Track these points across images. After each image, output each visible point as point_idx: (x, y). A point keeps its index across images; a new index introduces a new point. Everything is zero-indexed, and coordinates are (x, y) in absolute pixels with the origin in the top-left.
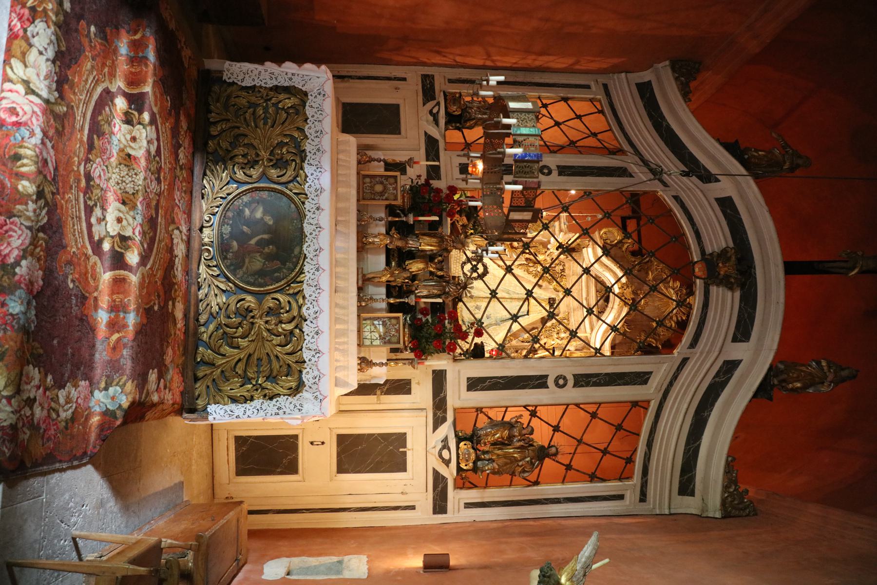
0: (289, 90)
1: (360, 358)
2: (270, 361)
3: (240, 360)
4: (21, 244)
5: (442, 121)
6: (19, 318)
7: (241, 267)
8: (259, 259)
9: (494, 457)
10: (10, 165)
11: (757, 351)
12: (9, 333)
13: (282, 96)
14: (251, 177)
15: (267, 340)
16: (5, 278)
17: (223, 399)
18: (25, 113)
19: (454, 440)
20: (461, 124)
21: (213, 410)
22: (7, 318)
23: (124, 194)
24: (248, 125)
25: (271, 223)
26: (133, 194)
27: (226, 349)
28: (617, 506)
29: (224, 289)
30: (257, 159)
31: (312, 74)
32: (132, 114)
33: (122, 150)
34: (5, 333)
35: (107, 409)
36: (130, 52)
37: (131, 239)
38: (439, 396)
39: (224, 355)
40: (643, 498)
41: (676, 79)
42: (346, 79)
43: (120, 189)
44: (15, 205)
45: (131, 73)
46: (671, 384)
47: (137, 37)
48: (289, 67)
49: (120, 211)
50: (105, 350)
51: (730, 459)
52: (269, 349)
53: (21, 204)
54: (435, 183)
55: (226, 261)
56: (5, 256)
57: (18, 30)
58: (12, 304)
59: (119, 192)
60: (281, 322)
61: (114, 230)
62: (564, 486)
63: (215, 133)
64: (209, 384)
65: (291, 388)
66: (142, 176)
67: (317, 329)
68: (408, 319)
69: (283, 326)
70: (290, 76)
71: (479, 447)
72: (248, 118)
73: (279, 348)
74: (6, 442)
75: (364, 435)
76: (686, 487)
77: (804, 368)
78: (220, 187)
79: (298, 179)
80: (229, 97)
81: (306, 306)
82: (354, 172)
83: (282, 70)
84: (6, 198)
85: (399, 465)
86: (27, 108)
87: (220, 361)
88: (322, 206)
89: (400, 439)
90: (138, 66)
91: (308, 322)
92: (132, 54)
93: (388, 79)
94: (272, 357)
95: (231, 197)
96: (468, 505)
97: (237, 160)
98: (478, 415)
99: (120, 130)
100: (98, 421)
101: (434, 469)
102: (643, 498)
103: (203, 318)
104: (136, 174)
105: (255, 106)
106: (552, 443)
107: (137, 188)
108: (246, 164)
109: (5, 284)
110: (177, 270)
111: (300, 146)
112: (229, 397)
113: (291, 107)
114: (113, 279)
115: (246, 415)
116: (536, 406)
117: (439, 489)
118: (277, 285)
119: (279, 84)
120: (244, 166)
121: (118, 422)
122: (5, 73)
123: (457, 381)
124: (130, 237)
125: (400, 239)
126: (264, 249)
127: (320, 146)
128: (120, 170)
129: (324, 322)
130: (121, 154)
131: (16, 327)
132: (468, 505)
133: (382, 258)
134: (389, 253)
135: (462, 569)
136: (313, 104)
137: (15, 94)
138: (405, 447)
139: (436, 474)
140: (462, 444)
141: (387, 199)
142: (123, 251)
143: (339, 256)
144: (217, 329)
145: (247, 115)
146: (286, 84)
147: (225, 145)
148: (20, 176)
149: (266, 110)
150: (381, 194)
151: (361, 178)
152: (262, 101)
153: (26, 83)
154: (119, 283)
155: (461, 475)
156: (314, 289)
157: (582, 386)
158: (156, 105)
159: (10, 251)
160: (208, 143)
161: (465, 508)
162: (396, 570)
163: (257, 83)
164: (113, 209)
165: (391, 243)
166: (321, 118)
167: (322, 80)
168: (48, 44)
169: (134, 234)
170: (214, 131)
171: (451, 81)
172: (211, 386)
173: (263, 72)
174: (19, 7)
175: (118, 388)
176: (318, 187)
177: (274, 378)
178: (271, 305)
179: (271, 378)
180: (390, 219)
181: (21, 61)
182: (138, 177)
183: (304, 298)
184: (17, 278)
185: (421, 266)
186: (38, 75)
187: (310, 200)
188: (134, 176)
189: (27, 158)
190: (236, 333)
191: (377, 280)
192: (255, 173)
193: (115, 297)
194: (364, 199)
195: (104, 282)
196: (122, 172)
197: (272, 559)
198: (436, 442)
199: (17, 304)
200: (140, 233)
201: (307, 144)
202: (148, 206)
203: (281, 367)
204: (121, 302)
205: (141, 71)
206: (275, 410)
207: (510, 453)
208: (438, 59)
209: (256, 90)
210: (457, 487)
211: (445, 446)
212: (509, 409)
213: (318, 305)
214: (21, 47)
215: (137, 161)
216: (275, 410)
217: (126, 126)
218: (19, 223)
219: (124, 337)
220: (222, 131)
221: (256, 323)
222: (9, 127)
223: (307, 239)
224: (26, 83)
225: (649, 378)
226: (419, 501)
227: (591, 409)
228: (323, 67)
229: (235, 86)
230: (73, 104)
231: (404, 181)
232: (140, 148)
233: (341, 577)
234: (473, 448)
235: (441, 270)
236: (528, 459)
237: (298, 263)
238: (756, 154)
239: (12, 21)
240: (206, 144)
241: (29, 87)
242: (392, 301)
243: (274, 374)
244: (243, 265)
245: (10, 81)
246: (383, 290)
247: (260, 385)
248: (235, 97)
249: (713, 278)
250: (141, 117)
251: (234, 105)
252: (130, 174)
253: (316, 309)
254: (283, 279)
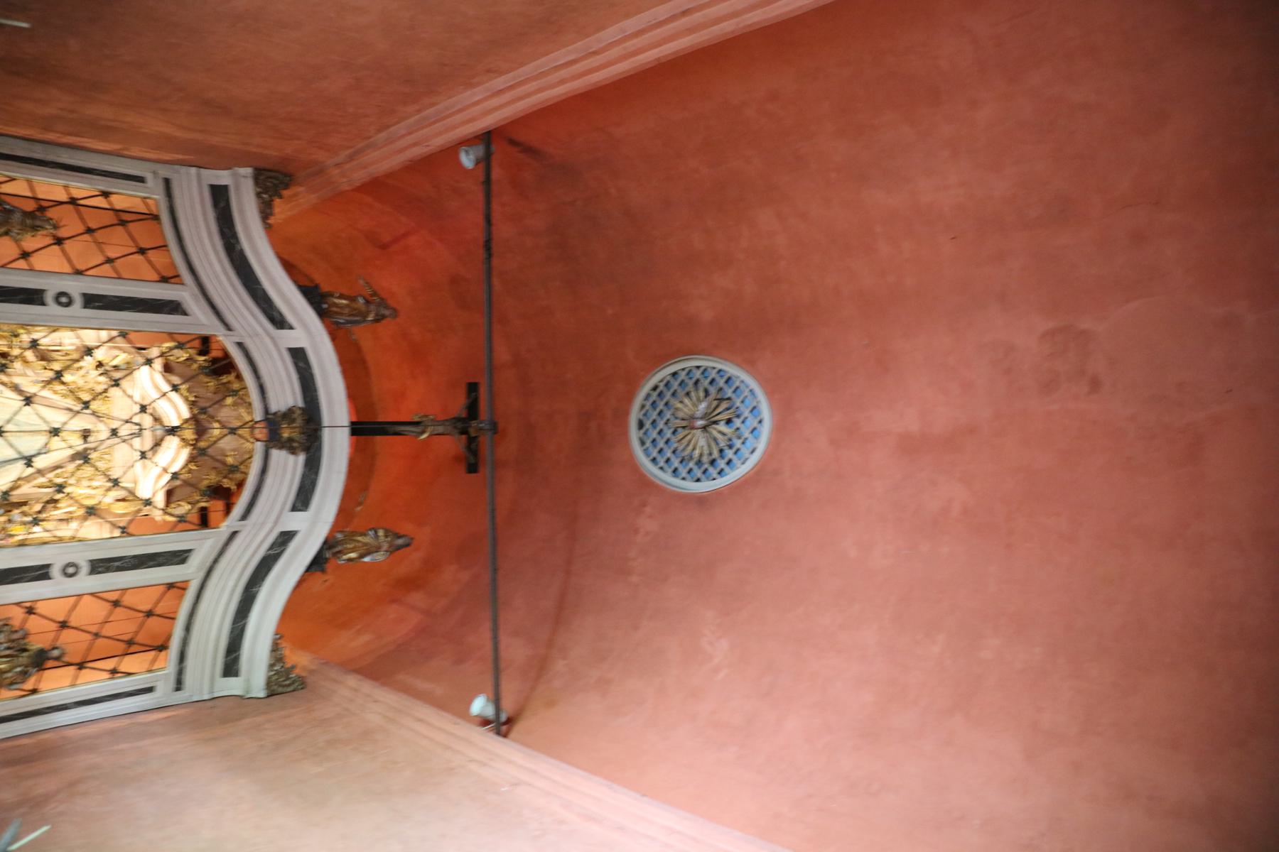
11: (314, 524)
28: (143, 701)
40: (179, 685)
41: (258, 195)
46: (216, 561)
51: (278, 636)
76: (231, 669)
77: (360, 538)
102: (179, 685)
157: (100, 573)
225: (187, 557)
227: (113, 596)
236: (19, 669)
238: (337, 301)
249: (274, 440)
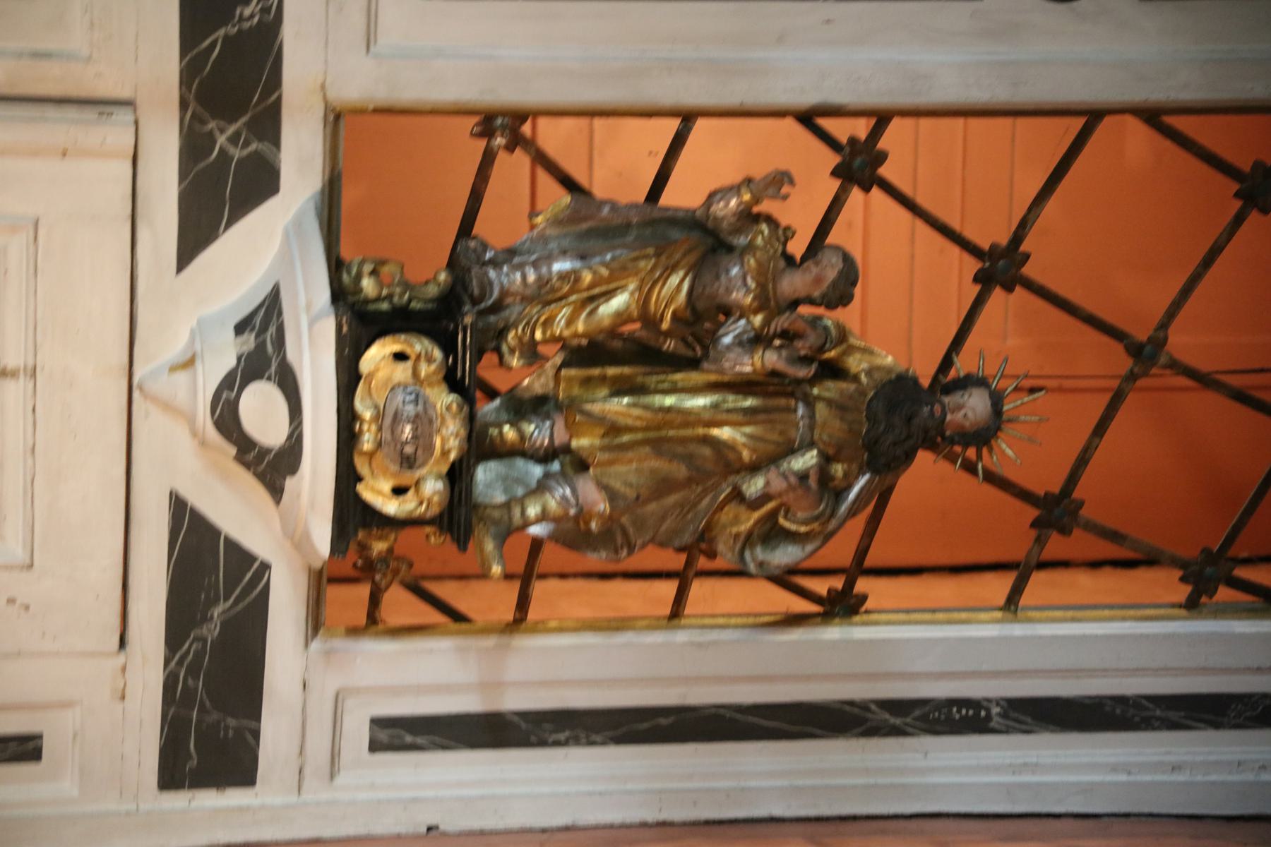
9: (582, 442)
19: (328, 329)
38: (226, 17)
62: (1017, 630)
71: (488, 370)
98: (488, 159)
101: (179, 506)
106: (963, 365)
116: (882, 119)
117: (211, 631)
140: (377, 355)
155: (364, 548)
161: (375, 746)
198: (201, 330)
207: (689, 418)
212: (701, 125)
226: (66, 705)
234: (453, 381)
236: (806, 461)
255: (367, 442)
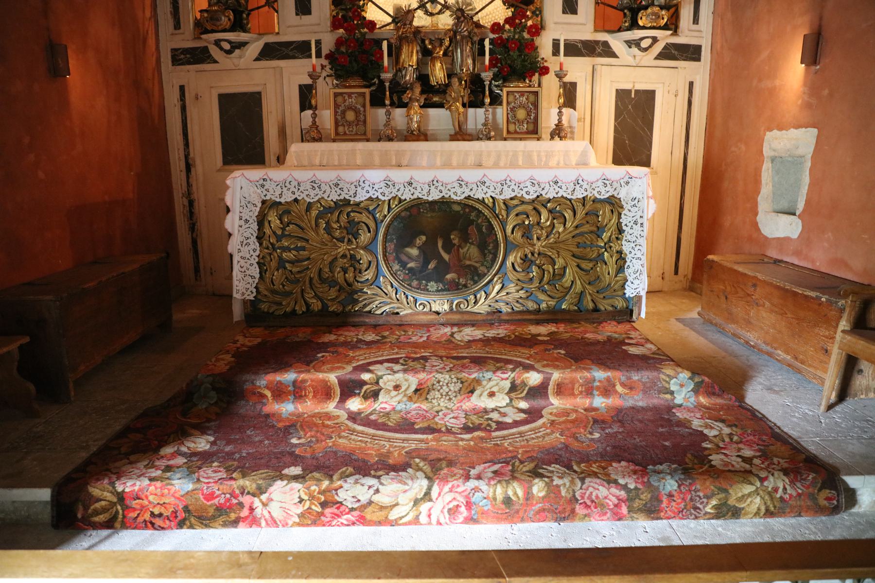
0: (261, 220)
1: (552, 138)
2: (581, 234)
3: (578, 266)
4: (604, 486)
5: (242, 36)
6: (679, 479)
7: (476, 268)
8: (467, 248)
10: (517, 507)
12: (698, 487)
13: (268, 231)
14: (370, 262)
15: (559, 238)
16: (642, 497)
17: (617, 281)
18: (454, 499)
19: (636, 31)
20: (243, 12)
21: (633, 291)
22: (683, 491)
23: (462, 392)
24: (308, 269)
25: (424, 238)
26: (462, 383)
27: (567, 280)
29: (500, 286)
30: (349, 256)
31: (238, 196)
32: (365, 392)
33: (410, 399)
34: (699, 491)
35: (692, 390)
36: (289, 400)
37: (514, 381)
39: (572, 282)
42: (190, 162)
43: (455, 397)
44: (562, 497)
45: (314, 396)
47: (268, 394)
48: (231, 223)
49: (481, 395)
50: (633, 397)
52: (567, 236)
53: (560, 491)
54: (328, 46)
55: (469, 285)
56: (619, 500)
57: (353, 516)
58: (668, 488)
59: (459, 397)
60: (538, 223)
61: (503, 398)
63: (319, 303)
64: (602, 296)
65: (612, 211)
66: (439, 376)
67: (551, 183)
68: (497, 83)
69: (542, 221)
70: (242, 223)
72: (298, 269)
73: (568, 225)
74: (803, 477)
75: (615, 137)
78: (384, 295)
79: (371, 208)
80: (274, 292)
81: (525, 196)
82: (335, 145)
83: (236, 232)
84: (556, 506)
85: (647, 98)
86: (449, 497)
87: (578, 287)
88: (408, 179)
89: (622, 95)
90: (305, 389)
91: (543, 193)
92: (291, 398)
93: (184, 108)
94: (577, 232)
95: (395, 284)
96: (696, 20)
97: (351, 280)
99: (386, 403)
100: (704, 397)
101: (656, 58)
103: (531, 306)
104: (439, 382)
105: (281, 264)
107: (455, 380)
108: (355, 269)
109: (649, 496)
110: (498, 334)
111: (330, 207)
112: (616, 276)
113: (280, 219)
114: (557, 395)
115: (642, 257)
117: (676, 53)
118: (497, 228)
119: (255, 235)
120: (358, 271)
121: (706, 379)
122: (409, 523)
123: (565, 26)
124: (511, 383)
125: (412, 89)
126: (455, 245)
127: (331, 184)
128: (434, 399)
129: (544, 176)
130: (415, 398)
131: (689, 481)
132: (696, 20)
133: (432, 111)
134: (428, 105)
135: (821, 19)
136: (277, 193)
137: (432, 511)
138: (630, 91)
139: (662, 56)
140: (641, 23)
141: (364, 106)
142: (527, 389)
143: (438, 162)
144: (544, 291)
145: (295, 270)
146: (255, 226)
147: (333, 293)
148: (528, 496)
149: (287, 249)
150: (357, 112)
151: (338, 137)
152: (276, 255)
153: (417, 502)
154: (561, 390)
156: (505, 187)
158: (344, 368)
159: (613, 496)
160: (333, 312)
161: (697, 24)
162: (806, 97)
163: (254, 260)
164: (480, 401)
165: (418, 101)
166: (294, 183)
167: (244, 182)
168: (363, 485)
169: (507, 379)
170: (316, 305)
171: (177, 26)
172: (604, 295)
173: (240, 254)
174: (322, 518)
175: (672, 382)
176: (383, 185)
177: (598, 228)
178: (519, 234)
179: (598, 233)
180: (387, 102)
181: (391, 510)
182: (442, 380)
183: (511, 199)
184: (640, 486)
185: (438, 65)
186: (405, 491)
187: (399, 194)
188: (441, 383)
189: (506, 491)
190: (549, 272)
191: (462, 118)
192: (364, 257)
193: (576, 392)
194: (365, 134)
195: (562, 404)
196: (436, 397)
197: (758, 230)
198: (629, 54)
199: (666, 483)
200: (504, 373)
201: (330, 199)
202: (464, 367)
203: (588, 222)
204: (582, 386)
205: (312, 386)
206: (638, 227)
208: (151, 42)
209: (262, 261)
210: (675, 32)
211: (637, 43)
213: (525, 181)
214: (374, 512)
215: (423, 382)
216: (638, 227)
217: (380, 397)
218: (581, 491)
219: (620, 379)
220: (316, 296)
221: (539, 250)
222: (473, 512)
223: (447, 196)
224: (417, 502)
228: (228, 182)
229: (259, 286)
230: (403, 452)
231: (325, 89)
232: (406, 380)
233: (810, 156)
235: (441, 41)
237: (472, 206)
239: (342, 523)
240: (335, 314)
241: (422, 499)
242: (487, 100)
243: (595, 229)
244: (473, 266)
245: (417, 517)
246: (471, 111)
247: (605, 244)
248: (274, 285)
250: (369, 382)
251: (284, 286)
252: (439, 388)
253: (528, 184)
254: (490, 222)
255: (655, 24)
